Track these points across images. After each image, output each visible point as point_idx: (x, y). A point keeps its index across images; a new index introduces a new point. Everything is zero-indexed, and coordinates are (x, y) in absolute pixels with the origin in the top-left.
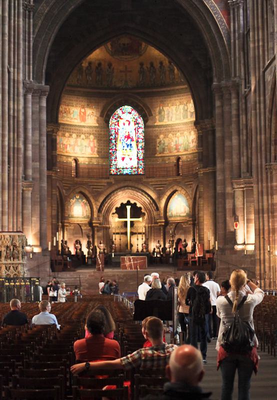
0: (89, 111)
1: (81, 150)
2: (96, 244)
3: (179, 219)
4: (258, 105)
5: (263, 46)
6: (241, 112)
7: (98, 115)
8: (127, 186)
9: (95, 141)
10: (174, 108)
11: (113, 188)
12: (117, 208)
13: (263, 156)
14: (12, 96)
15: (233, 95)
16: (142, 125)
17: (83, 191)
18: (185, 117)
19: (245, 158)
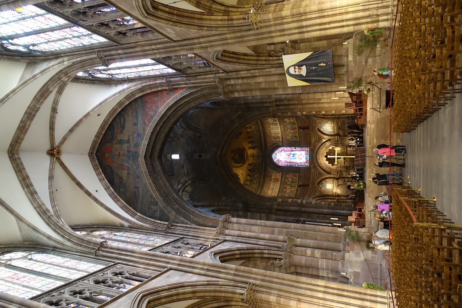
0: (273, 177)
1: (294, 182)
2: (350, 176)
3: (335, 128)
4: (203, 45)
5: (155, 44)
6: (239, 76)
7: (276, 172)
8: (316, 157)
9: (290, 174)
10: (272, 131)
11: (317, 165)
12: (329, 163)
13: (245, 33)
14: (189, 269)
15: (228, 82)
16: (282, 148)
17: (317, 182)
18: (276, 124)
19: (272, 69)
